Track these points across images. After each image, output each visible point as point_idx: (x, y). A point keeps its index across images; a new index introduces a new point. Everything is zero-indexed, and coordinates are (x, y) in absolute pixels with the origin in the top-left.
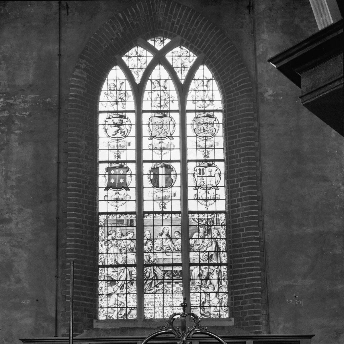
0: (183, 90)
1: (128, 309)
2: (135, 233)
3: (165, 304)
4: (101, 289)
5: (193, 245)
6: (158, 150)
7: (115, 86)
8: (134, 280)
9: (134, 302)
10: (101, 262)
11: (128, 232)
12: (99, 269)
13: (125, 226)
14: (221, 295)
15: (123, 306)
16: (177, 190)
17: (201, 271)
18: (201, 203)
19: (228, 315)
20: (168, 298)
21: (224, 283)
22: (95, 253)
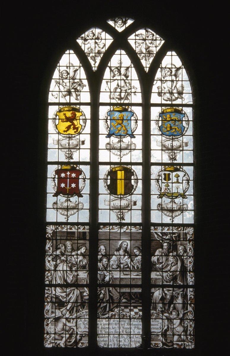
0: (147, 80)
1: (79, 335)
2: (88, 248)
3: (121, 331)
4: (47, 311)
5: (155, 264)
6: (116, 151)
7: (68, 74)
8: (85, 302)
9: (85, 327)
10: (47, 280)
11: (79, 246)
12: (45, 289)
13: (76, 238)
14: (187, 322)
15: (73, 332)
16: (137, 197)
17: (164, 294)
18: (165, 215)
19: (194, 345)
20: (124, 325)
21: (191, 308)
22: (43, 269)
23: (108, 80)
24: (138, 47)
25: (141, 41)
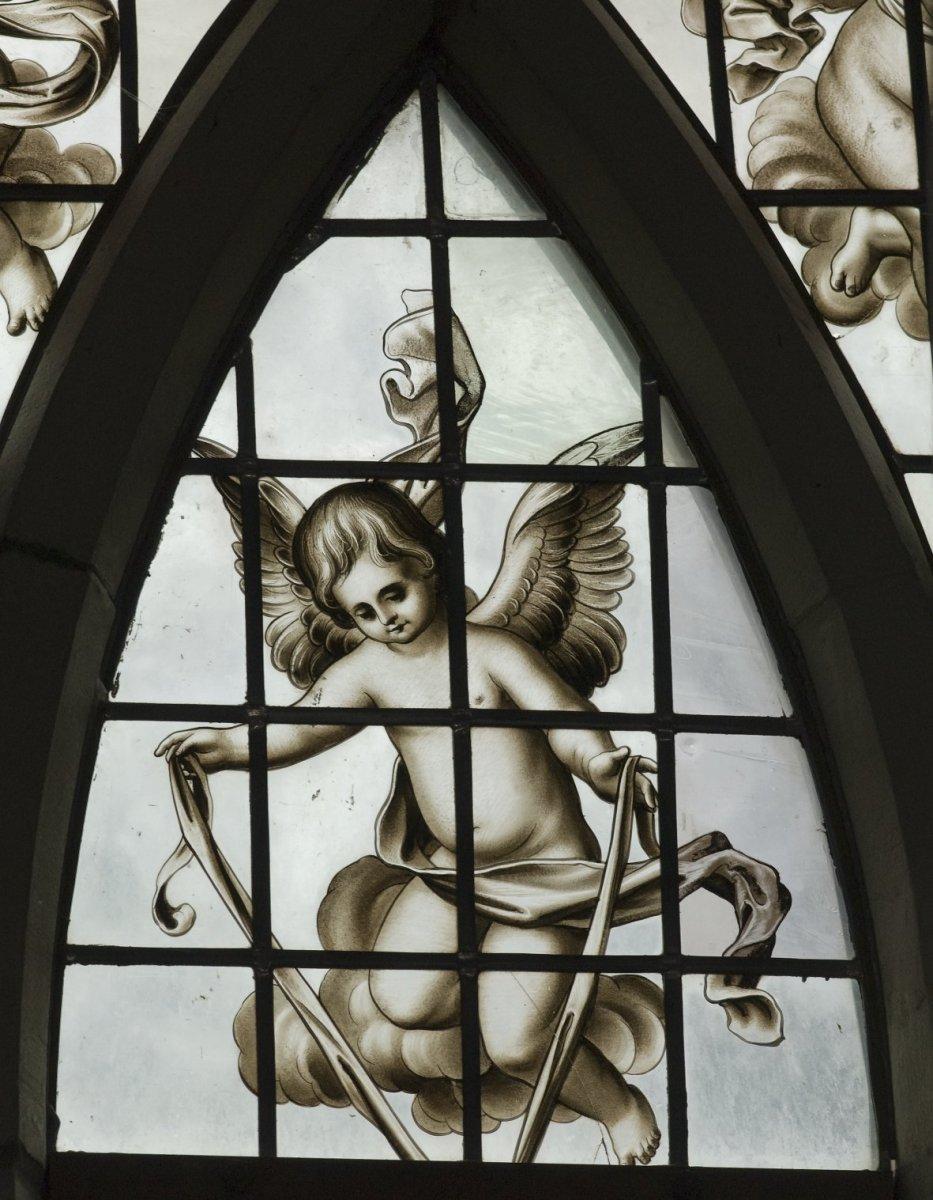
23: (200, 734)
24: (759, 76)
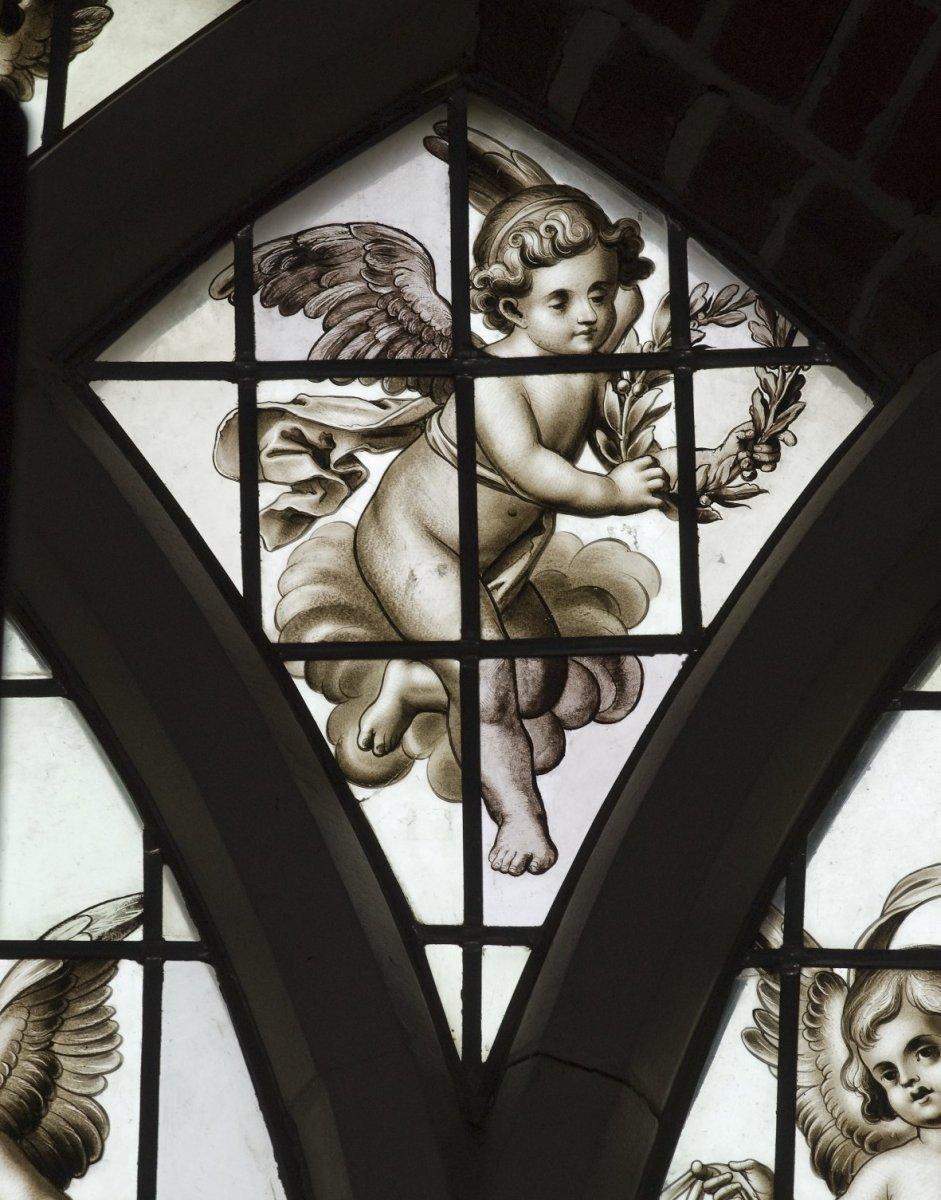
24: (294, 521)
25: (356, 404)
